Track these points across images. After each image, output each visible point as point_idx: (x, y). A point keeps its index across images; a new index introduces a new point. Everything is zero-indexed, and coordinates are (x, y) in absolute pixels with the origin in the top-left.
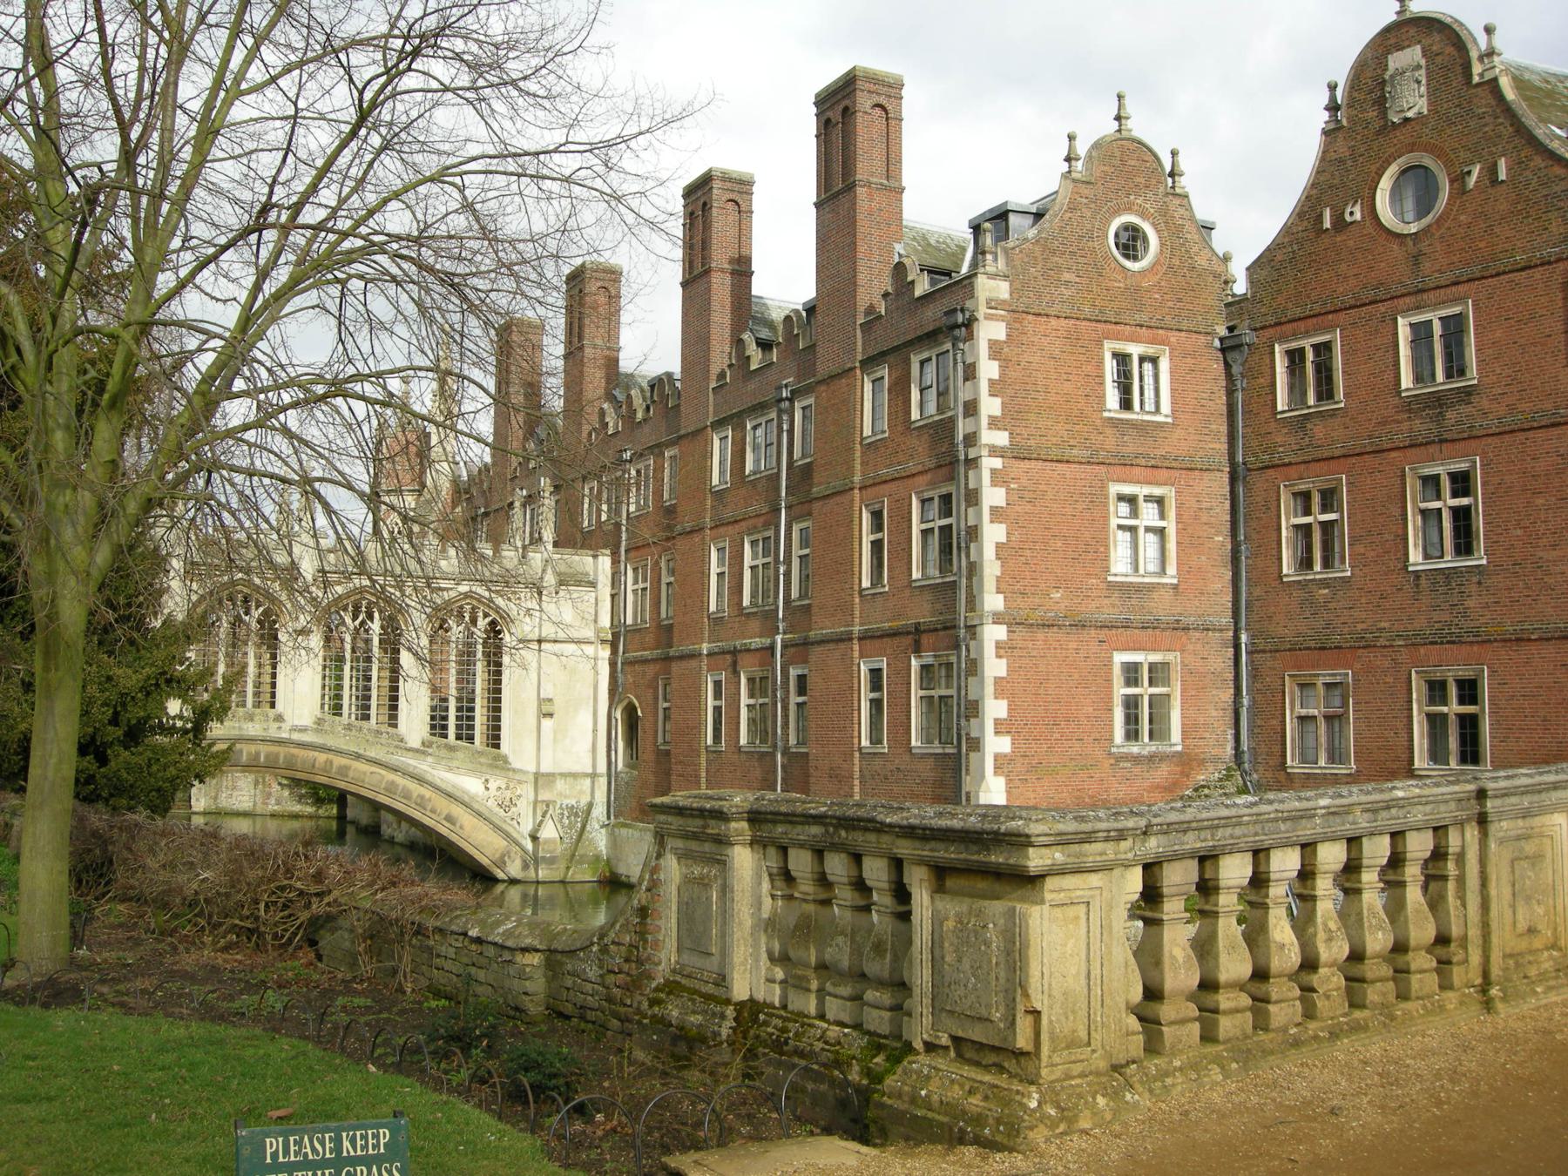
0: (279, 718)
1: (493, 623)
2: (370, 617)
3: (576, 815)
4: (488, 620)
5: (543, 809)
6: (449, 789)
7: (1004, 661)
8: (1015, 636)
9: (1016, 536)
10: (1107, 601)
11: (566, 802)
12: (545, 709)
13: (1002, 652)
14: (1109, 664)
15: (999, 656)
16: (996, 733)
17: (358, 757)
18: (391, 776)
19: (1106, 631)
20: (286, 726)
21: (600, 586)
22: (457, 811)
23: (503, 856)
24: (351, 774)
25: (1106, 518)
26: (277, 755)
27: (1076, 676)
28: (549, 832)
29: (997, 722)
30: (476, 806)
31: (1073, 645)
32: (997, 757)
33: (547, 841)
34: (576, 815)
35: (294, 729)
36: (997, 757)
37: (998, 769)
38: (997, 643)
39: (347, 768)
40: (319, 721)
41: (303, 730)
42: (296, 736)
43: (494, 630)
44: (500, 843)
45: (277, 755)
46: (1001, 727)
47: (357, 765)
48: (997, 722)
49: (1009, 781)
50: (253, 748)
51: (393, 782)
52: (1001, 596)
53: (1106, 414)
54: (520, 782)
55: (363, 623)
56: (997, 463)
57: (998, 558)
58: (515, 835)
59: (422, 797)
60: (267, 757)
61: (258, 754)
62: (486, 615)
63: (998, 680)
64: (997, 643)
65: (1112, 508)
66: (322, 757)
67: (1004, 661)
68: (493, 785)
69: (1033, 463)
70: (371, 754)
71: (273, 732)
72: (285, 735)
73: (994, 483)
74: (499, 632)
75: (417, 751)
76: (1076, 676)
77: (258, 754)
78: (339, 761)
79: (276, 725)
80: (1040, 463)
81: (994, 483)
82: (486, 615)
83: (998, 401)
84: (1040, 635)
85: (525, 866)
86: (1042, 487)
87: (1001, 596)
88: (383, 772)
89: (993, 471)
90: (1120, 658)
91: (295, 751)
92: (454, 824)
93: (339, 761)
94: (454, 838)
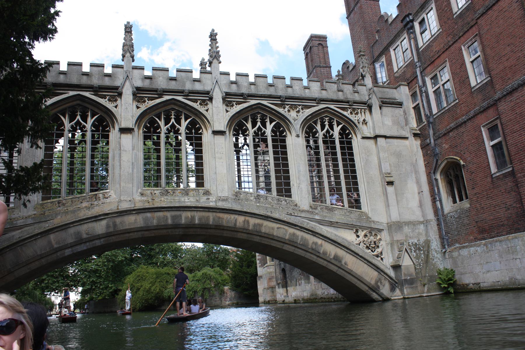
0: (207, 193)
1: (343, 129)
2: (264, 124)
3: (419, 249)
4: (340, 126)
5: (401, 247)
6: (333, 238)
11: (411, 241)
12: (388, 179)
18: (291, 230)
20: (212, 198)
21: (405, 104)
22: (341, 253)
23: (377, 282)
26: (208, 218)
28: (406, 262)
30: (353, 248)
33: (407, 267)
34: (419, 249)
39: (261, 225)
41: (225, 200)
42: (220, 205)
43: (344, 133)
44: (375, 274)
47: (266, 223)
50: (189, 214)
51: (294, 234)
54: (380, 231)
58: (382, 267)
59: (316, 244)
60: (200, 219)
61: (193, 218)
62: (338, 124)
66: (241, 219)
68: (361, 233)
70: (276, 215)
71: (203, 202)
72: (212, 204)
74: (350, 133)
75: (308, 211)
77: (193, 218)
79: (205, 198)
82: (338, 124)
85: (393, 289)
92: (340, 261)
93: (253, 221)
94: (340, 272)
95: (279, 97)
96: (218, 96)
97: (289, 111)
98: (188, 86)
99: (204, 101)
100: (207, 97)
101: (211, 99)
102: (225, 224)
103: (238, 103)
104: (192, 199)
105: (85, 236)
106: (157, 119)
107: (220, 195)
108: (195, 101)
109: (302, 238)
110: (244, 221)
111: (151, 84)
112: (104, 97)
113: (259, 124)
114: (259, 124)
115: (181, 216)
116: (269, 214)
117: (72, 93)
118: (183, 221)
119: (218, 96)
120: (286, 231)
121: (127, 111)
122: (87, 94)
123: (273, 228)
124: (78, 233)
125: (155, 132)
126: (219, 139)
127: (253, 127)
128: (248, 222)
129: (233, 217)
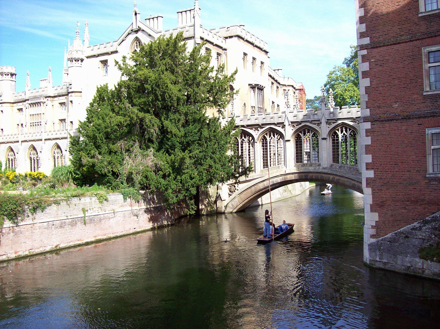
0: (319, 165)
7: (370, 137)
8: (374, 126)
9: (375, 82)
10: (423, 105)
13: (369, 134)
14: (424, 135)
15: (367, 136)
16: (367, 169)
17: (342, 177)
18: (353, 182)
19: (422, 119)
24: (341, 181)
25: (421, 65)
26: (318, 176)
27: (406, 142)
29: (367, 164)
31: (404, 128)
32: (367, 179)
35: (324, 168)
36: (367, 179)
37: (368, 185)
38: (366, 130)
39: (339, 180)
40: (332, 166)
42: (324, 171)
45: (318, 176)
46: (368, 167)
47: (342, 179)
48: (367, 164)
49: (373, 190)
50: (311, 175)
51: (354, 184)
52: (368, 110)
53: (420, 15)
55: (344, 134)
56: (365, 52)
57: (366, 94)
60: (315, 177)
63: (367, 146)
64: (366, 130)
65: (424, 59)
66: (331, 177)
67: (370, 137)
69: (382, 49)
70: (347, 176)
72: (320, 170)
73: (363, 61)
76: (406, 142)
78: (337, 178)
80: (385, 48)
81: (363, 61)
83: (364, 25)
84: (387, 124)
86: (386, 58)
87: (368, 110)
88: (351, 181)
89: (363, 56)
90: (429, 131)
91: (323, 175)
93: (337, 178)
95: (352, 118)
96: (323, 121)
97: (358, 124)
98: (312, 118)
99: (318, 124)
100: (319, 122)
101: (321, 123)
102: (325, 179)
103: (334, 123)
104: (313, 168)
105: (275, 183)
106: (300, 134)
107: (324, 166)
108: (315, 124)
109: (358, 185)
110: (333, 178)
111: (297, 119)
112: (279, 126)
113: (344, 132)
114: (344, 132)
115: (307, 175)
116: (344, 175)
117: (268, 127)
118: (309, 177)
119: (323, 121)
120: (351, 182)
121: (289, 132)
122: (273, 126)
123: (345, 181)
124: (273, 182)
125: (300, 139)
126: (324, 141)
127: (342, 133)
128: (334, 178)
129: (328, 175)
